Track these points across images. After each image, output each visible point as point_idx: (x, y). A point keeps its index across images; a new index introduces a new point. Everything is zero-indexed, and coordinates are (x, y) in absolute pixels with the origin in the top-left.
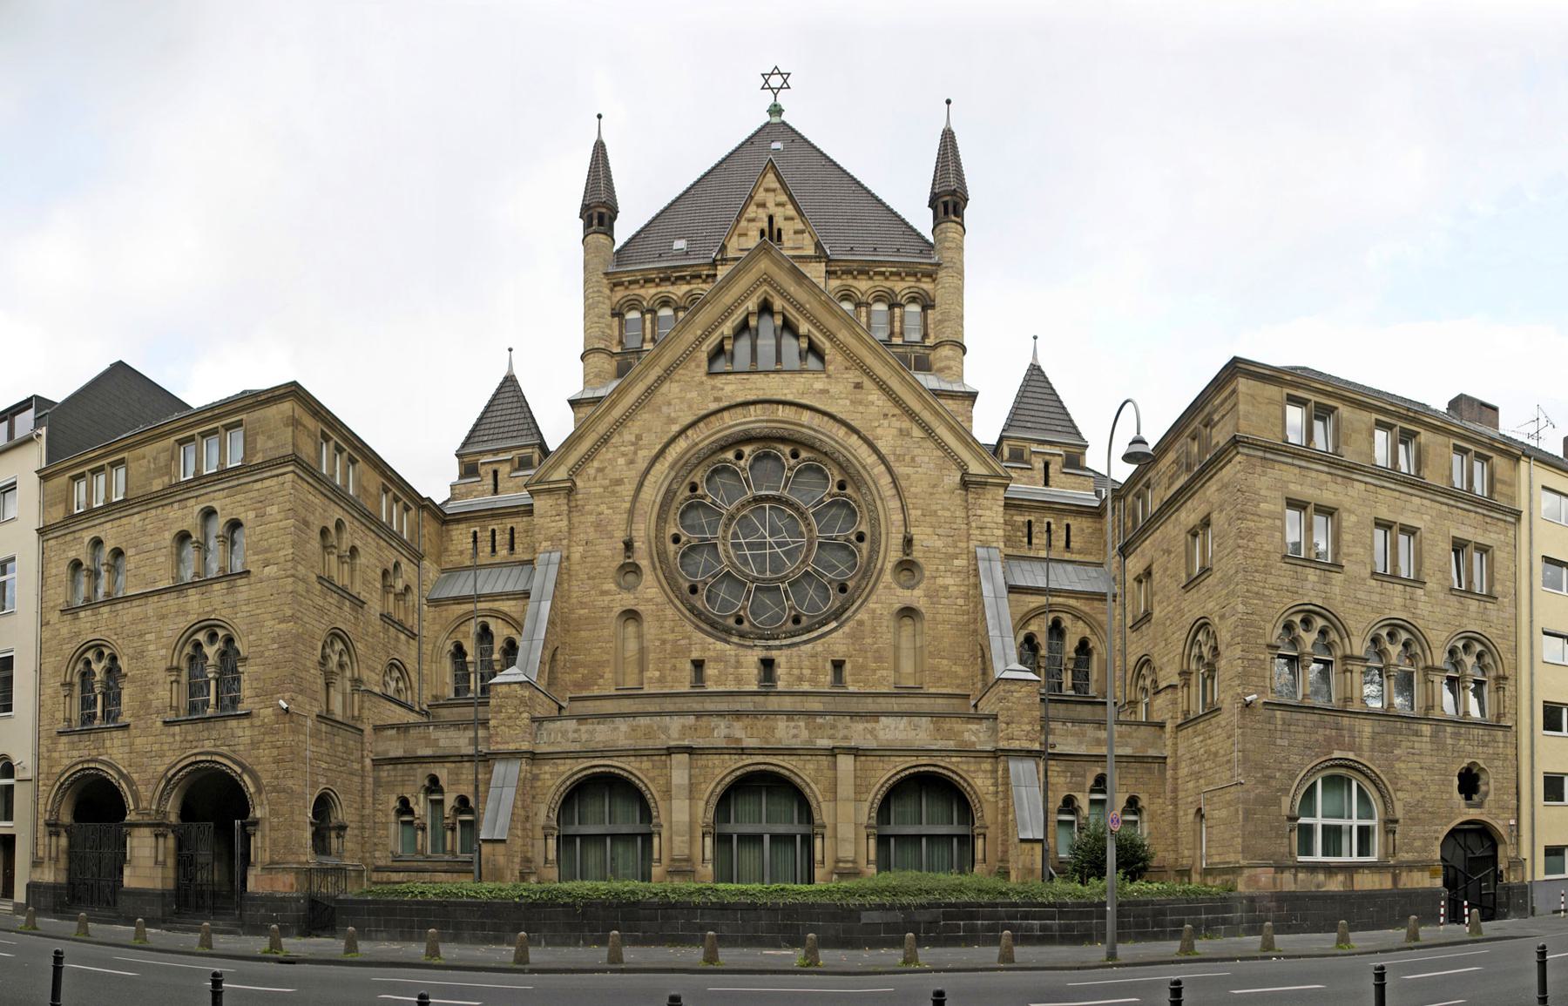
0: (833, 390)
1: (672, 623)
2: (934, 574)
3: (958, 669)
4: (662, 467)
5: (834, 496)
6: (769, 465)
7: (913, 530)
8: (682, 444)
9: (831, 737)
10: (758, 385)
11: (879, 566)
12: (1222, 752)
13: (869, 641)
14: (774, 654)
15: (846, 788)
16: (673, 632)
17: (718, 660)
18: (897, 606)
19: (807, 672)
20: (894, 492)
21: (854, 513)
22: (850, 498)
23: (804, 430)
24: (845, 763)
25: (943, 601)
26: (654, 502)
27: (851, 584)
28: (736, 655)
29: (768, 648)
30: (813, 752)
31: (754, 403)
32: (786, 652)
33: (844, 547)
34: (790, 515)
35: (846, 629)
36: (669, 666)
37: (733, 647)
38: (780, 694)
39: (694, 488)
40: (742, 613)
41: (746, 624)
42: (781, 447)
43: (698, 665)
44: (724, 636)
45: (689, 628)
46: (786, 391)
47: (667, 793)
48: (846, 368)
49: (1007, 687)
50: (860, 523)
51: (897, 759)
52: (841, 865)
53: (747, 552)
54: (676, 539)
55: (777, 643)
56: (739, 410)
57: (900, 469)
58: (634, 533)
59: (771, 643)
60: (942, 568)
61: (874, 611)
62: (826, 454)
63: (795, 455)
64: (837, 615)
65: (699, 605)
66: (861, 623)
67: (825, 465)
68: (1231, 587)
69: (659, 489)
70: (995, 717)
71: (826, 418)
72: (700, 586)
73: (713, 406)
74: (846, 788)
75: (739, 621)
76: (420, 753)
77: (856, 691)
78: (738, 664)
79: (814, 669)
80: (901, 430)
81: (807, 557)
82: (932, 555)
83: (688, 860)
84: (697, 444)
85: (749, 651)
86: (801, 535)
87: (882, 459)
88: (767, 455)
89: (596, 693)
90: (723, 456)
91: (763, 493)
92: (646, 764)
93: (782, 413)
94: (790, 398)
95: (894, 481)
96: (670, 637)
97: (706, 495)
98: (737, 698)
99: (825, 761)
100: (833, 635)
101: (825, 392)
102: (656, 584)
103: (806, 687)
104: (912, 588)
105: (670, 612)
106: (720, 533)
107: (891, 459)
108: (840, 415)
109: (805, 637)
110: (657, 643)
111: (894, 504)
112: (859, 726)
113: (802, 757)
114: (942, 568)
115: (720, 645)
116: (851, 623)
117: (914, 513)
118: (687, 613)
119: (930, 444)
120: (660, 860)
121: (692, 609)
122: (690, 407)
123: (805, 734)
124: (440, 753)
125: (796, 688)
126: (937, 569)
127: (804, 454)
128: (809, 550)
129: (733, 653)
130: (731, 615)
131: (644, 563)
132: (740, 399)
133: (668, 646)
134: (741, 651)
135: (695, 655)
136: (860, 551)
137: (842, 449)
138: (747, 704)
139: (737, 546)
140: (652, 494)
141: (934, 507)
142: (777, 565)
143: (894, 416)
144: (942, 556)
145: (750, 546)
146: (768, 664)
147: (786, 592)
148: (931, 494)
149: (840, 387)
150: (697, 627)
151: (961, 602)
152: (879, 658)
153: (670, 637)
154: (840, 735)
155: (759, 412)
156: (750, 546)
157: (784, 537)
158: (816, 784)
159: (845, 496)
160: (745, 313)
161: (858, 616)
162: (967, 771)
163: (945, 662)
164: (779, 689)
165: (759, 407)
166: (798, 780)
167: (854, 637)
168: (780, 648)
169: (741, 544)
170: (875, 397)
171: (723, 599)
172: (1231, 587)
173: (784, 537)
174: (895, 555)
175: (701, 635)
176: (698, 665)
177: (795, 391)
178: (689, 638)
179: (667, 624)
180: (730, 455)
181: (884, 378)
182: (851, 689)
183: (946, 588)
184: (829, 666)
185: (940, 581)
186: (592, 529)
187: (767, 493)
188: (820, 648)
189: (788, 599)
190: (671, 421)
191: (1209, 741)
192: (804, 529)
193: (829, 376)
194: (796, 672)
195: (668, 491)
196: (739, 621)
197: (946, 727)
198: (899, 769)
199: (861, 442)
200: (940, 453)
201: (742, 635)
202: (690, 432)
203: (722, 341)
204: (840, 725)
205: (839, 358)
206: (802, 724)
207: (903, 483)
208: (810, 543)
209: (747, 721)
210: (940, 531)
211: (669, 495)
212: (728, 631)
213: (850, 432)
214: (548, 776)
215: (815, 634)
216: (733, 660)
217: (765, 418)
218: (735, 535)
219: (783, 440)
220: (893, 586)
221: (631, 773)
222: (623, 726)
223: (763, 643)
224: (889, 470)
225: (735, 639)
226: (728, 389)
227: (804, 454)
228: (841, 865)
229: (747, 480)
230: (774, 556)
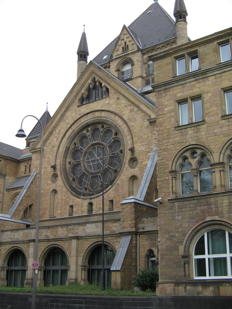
0: (111, 102)
1: (65, 193)
2: (142, 161)
4: (65, 140)
5: (113, 139)
8: (70, 131)
10: (91, 107)
13: (120, 191)
16: (65, 196)
17: (77, 205)
18: (130, 176)
23: (103, 118)
26: (62, 151)
28: (82, 203)
31: (89, 113)
32: (96, 199)
35: (114, 188)
37: (81, 200)
38: (93, 215)
39: (75, 144)
42: (98, 125)
43: (72, 207)
44: (78, 196)
45: (69, 194)
46: (98, 107)
48: (115, 94)
51: (91, 240)
53: (91, 164)
54: (70, 162)
55: (94, 196)
56: (86, 116)
57: (130, 124)
58: (57, 163)
59: (92, 197)
66: (118, 185)
67: (111, 128)
69: (64, 147)
73: (79, 117)
77: (117, 211)
78: (82, 206)
80: (131, 110)
82: (141, 153)
84: (74, 130)
87: (125, 122)
89: (44, 219)
90: (83, 132)
93: (97, 114)
94: (99, 109)
97: (79, 147)
98: (81, 218)
101: (109, 103)
102: (61, 180)
105: (65, 189)
106: (82, 159)
107: (127, 121)
111: (129, 137)
112: (81, 228)
113: (65, 241)
115: (78, 200)
116: (115, 185)
119: (140, 112)
121: (71, 187)
122: (73, 118)
123: (66, 233)
126: (143, 158)
129: (81, 202)
131: (59, 173)
132: (86, 113)
134: (83, 201)
135: (71, 204)
138: (84, 220)
139: (89, 162)
140: (62, 149)
141: (141, 135)
143: (128, 105)
144: (144, 153)
146: (91, 204)
148: (141, 130)
149: (113, 101)
150: (72, 194)
153: (64, 198)
155: (90, 116)
156: (93, 161)
158: (68, 251)
160: (89, 84)
162: (113, 243)
164: (93, 214)
165: (91, 114)
167: (116, 190)
168: (94, 198)
169: (90, 161)
170: (123, 101)
174: (128, 156)
176: (72, 207)
177: (100, 106)
178: (69, 198)
179: (64, 193)
180: (85, 132)
181: (124, 94)
186: (47, 163)
189: (100, 179)
190: (68, 124)
194: (98, 206)
195: (66, 147)
198: (91, 243)
200: (143, 114)
202: (72, 127)
203: (83, 95)
204: (75, 228)
206: (65, 229)
207: (131, 129)
209: (51, 229)
211: (68, 149)
213: (115, 115)
216: (81, 204)
217: (92, 117)
218: (88, 159)
220: (129, 168)
225: (82, 197)
226: (83, 110)
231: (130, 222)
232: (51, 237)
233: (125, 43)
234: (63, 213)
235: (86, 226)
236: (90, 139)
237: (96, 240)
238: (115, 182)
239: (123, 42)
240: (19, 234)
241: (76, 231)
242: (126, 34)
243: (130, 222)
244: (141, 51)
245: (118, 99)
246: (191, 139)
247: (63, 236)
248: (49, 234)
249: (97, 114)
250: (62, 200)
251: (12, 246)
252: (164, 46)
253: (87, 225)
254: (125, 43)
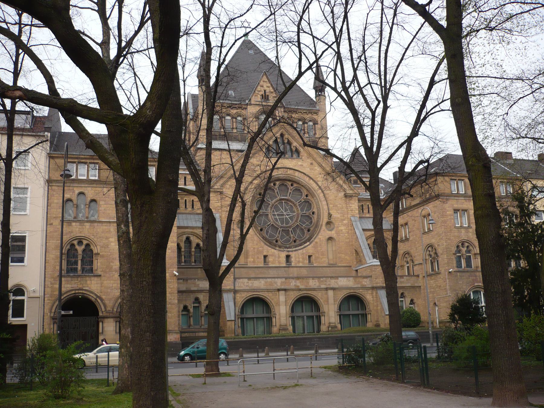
0: (305, 165)
3: (347, 257)
6: (283, 187)
7: (331, 212)
9: (325, 284)
11: (321, 223)
12: (442, 286)
14: (290, 253)
15: (331, 301)
17: (272, 255)
18: (327, 237)
19: (301, 260)
20: (324, 199)
21: (310, 204)
22: (310, 200)
24: (331, 293)
25: (341, 235)
27: (312, 229)
29: (288, 251)
30: (320, 289)
32: (294, 253)
33: (308, 216)
34: (291, 205)
35: (312, 245)
36: (256, 257)
40: (278, 239)
41: (279, 243)
42: (288, 182)
43: (265, 257)
45: (262, 244)
47: (278, 304)
49: (375, 267)
50: (313, 208)
52: (331, 324)
55: (291, 249)
59: (289, 250)
60: (340, 224)
61: (320, 238)
62: (303, 186)
63: (292, 185)
64: (309, 240)
65: (264, 235)
66: (316, 243)
68: (441, 237)
70: (371, 277)
71: (303, 174)
72: (264, 229)
74: (331, 301)
75: (277, 241)
76: (192, 289)
78: (279, 257)
79: (303, 259)
81: (297, 219)
83: (286, 325)
85: (282, 252)
86: (294, 212)
88: (283, 184)
91: (283, 197)
92: (270, 294)
93: (290, 172)
94: (291, 167)
95: (324, 195)
96: (256, 247)
98: (279, 269)
99: (324, 292)
100: (309, 247)
101: (302, 165)
103: (301, 265)
104: (331, 230)
105: (256, 238)
106: (269, 211)
108: (307, 174)
109: (300, 248)
110: (252, 249)
111: (324, 203)
114: (340, 224)
115: (273, 250)
116: (314, 243)
117: (331, 206)
118: (261, 239)
120: (276, 326)
121: (263, 238)
123: (317, 284)
124: (200, 289)
125: (298, 265)
127: (295, 185)
128: (298, 217)
130: (274, 240)
133: (256, 250)
134: (280, 253)
135: (265, 254)
136: (314, 218)
137: (308, 185)
139: (274, 215)
141: (336, 204)
142: (287, 222)
145: (278, 215)
146: (288, 257)
147: (291, 231)
150: (265, 244)
151: (346, 235)
152: (323, 255)
154: (328, 284)
156: (278, 215)
157: (289, 212)
159: (308, 199)
161: (316, 240)
163: (343, 255)
166: (316, 299)
167: (315, 247)
168: (292, 251)
171: (270, 233)
172: (441, 237)
173: (289, 212)
174: (325, 219)
175: (267, 247)
179: (255, 242)
182: (315, 265)
183: (342, 230)
184: (307, 257)
185: (340, 228)
187: (284, 198)
188: (304, 252)
191: (437, 282)
192: (295, 210)
193: (303, 160)
194: (297, 259)
196: (277, 241)
197: (357, 280)
199: (313, 182)
201: (280, 247)
205: (305, 155)
206: (317, 281)
207: (327, 196)
208: (298, 215)
209: (301, 280)
210: (339, 212)
212: (275, 246)
214: (238, 298)
215: (303, 247)
216: (277, 255)
219: (289, 181)
220: (326, 230)
221: (265, 297)
222: (263, 281)
223: (287, 249)
224: (323, 192)
225: (277, 248)
227: (295, 185)
228: (331, 324)
229: (277, 192)
230: (286, 218)
231: (381, 280)
232: (302, 287)
233: (265, 91)
234: (256, 262)
235: (338, 279)
236: (277, 192)
237: (349, 291)
238: (313, 239)
239: (262, 89)
240: (260, 282)
241: (328, 283)
242: (266, 82)
243: (381, 280)
244: (284, 108)
245: (312, 164)
246: (464, 236)
247: (315, 287)
248: (299, 284)
249: (290, 172)
250: (254, 248)
251: (252, 294)
252: (306, 113)
253: (339, 278)
254: (265, 91)
